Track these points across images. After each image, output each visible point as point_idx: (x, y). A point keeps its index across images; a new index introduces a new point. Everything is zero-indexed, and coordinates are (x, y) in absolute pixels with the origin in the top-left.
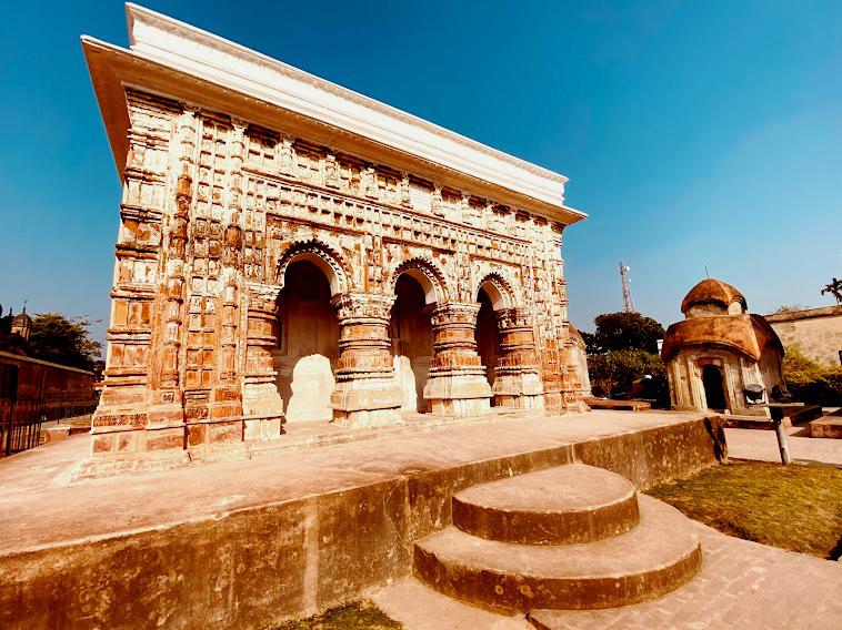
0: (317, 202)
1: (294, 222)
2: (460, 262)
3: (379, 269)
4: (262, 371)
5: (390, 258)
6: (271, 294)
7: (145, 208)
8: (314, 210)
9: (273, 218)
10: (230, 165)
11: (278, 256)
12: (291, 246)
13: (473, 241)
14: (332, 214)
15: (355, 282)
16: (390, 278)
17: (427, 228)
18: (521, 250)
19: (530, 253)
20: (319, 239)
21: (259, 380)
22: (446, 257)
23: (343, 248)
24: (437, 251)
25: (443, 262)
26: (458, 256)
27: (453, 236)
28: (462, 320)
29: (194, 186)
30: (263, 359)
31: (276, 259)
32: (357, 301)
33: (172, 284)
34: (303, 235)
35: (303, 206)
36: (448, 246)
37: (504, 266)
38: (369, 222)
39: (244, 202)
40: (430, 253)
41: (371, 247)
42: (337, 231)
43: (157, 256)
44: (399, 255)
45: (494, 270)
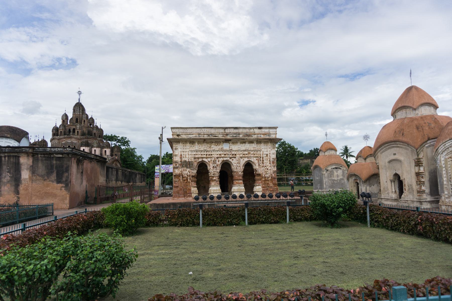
0: (203, 153)
1: (198, 158)
8: (202, 155)
9: (195, 158)
10: (187, 150)
11: (196, 165)
17: (228, 153)
19: (261, 153)
21: (195, 187)
22: (233, 159)
24: (231, 158)
27: (235, 153)
34: (200, 160)
36: (234, 156)
39: (190, 156)
42: (207, 158)
45: (249, 159)
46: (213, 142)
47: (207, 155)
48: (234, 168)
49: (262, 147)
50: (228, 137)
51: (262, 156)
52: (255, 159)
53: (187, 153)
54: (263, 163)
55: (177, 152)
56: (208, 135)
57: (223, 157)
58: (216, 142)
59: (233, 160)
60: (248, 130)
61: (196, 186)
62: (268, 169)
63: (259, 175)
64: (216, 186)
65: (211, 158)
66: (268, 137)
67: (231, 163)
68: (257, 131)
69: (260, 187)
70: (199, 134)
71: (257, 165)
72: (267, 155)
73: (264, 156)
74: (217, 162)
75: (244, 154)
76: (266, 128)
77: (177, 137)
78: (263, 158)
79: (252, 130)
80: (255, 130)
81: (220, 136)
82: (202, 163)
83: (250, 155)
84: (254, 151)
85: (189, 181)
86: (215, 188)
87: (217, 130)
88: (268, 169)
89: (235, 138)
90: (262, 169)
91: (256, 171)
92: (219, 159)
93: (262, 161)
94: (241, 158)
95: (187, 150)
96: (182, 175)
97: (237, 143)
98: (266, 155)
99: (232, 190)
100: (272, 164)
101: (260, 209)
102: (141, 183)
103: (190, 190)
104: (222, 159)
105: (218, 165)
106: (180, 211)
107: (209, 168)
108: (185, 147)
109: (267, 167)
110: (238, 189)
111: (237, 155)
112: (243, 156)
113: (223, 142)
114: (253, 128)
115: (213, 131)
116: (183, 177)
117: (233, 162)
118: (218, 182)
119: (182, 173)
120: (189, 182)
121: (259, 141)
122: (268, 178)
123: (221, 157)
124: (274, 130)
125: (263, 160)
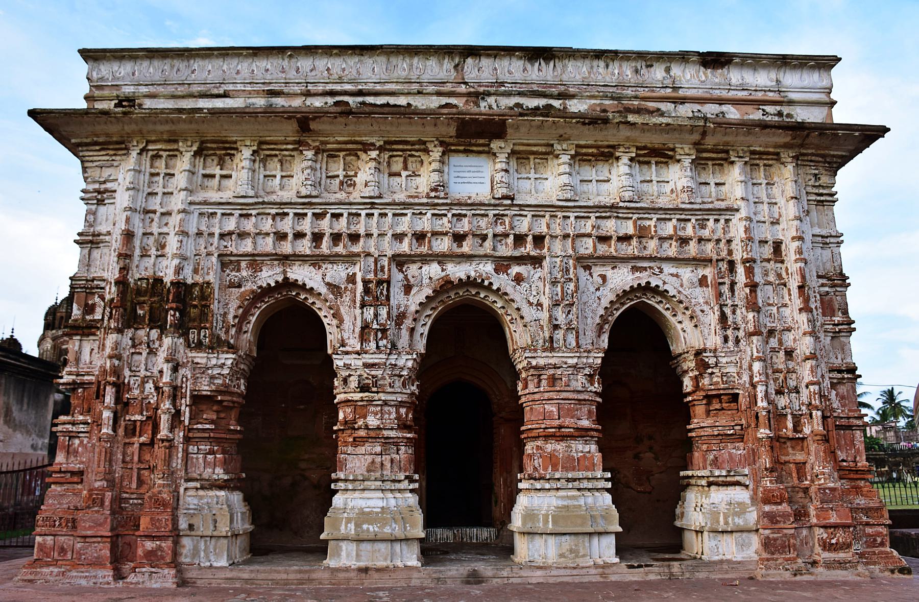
1: (256, 261)
3: (383, 312)
5: (408, 289)
10: (177, 202)
12: (253, 292)
13: (588, 230)
15: (346, 336)
16: (408, 322)
20: (292, 276)
23: (328, 284)
29: (137, 243)
31: (230, 317)
32: (347, 367)
34: (269, 276)
36: (529, 248)
37: (668, 268)
40: (488, 268)
41: (371, 276)
42: (316, 261)
45: (643, 278)
46: (366, 147)
52: (687, 273)
57: (442, 258)
59: (519, 279)
60: (625, 72)
61: (220, 474)
64: (387, 485)
68: (691, 78)
69: (741, 495)
72: (777, 246)
74: (397, 297)
76: (755, 61)
78: (749, 272)
80: (677, 70)
85: (164, 432)
86: (373, 501)
87: (403, 67)
88: (789, 354)
91: (703, 366)
92: (413, 269)
94: (585, 262)
96: (120, 388)
98: (768, 251)
99: (517, 522)
104: (434, 270)
107: (332, 336)
110: (561, 515)
112: (602, 249)
115: (371, 72)
116: (122, 405)
117: (517, 294)
118: (404, 453)
119: (116, 371)
121: (712, 146)
123: (425, 259)
124: (812, 79)
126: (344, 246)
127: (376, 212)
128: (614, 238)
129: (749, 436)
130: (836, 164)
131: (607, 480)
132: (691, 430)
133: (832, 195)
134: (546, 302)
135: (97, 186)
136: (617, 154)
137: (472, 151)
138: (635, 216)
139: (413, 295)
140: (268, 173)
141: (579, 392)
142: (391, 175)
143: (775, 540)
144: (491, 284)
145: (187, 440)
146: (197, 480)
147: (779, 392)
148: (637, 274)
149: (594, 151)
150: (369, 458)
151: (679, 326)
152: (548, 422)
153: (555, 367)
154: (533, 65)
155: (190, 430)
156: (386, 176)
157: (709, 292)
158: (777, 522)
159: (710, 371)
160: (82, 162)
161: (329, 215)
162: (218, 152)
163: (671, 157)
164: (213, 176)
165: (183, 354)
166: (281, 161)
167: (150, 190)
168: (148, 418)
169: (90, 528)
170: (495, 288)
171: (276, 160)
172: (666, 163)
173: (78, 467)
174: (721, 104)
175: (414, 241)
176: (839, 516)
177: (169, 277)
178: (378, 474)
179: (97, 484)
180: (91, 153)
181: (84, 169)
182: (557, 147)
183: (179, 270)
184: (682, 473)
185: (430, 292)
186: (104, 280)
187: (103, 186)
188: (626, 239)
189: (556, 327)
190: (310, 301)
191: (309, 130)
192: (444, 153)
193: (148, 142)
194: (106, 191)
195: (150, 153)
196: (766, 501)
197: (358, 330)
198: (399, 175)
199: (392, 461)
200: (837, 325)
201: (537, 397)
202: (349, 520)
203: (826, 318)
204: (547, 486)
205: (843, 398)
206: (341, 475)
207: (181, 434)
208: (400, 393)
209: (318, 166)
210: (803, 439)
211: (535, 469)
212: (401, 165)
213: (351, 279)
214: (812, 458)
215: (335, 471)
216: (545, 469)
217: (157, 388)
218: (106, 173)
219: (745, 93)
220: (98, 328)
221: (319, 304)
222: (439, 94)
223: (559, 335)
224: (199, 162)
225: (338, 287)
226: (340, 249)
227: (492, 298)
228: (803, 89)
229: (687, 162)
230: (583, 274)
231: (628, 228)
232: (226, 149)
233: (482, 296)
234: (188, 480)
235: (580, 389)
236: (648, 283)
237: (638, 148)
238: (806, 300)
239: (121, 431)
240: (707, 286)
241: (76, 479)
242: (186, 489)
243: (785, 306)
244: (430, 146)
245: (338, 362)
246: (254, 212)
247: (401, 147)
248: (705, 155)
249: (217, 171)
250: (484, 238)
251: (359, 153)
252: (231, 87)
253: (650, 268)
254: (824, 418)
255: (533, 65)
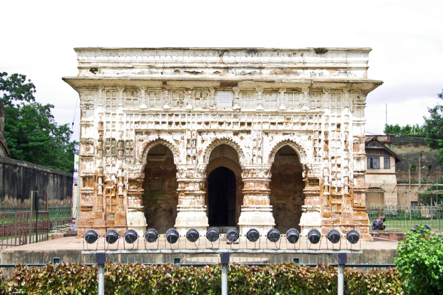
0: (160, 119)
1: (148, 133)
2: (255, 137)
3: (194, 151)
4: (135, 206)
5: (203, 141)
6: (138, 169)
7: (88, 138)
8: (157, 123)
11: (141, 150)
12: (147, 143)
14: (167, 123)
16: (203, 154)
18: (315, 120)
19: (323, 120)
23: (175, 140)
24: (236, 133)
25: (242, 138)
26: (254, 134)
27: (249, 120)
28: (254, 176)
29: (105, 124)
30: (136, 201)
32: (182, 170)
33: (99, 170)
34: (153, 137)
35: (152, 122)
36: (246, 127)
38: (189, 123)
39: (125, 127)
41: (189, 138)
42: (170, 132)
43: (93, 158)
44: (209, 138)
45: (287, 137)
46: (187, 89)
47: (170, 123)
48: (245, 161)
49: (326, 104)
50: (230, 76)
51: (323, 130)
53: (117, 117)
54: (327, 150)
55: (95, 116)
56: (176, 70)
57: (214, 132)
58: (195, 89)
61: (139, 206)
62: (339, 166)
63: (315, 181)
65: (182, 131)
66: (341, 76)
67: (238, 146)
70: (151, 67)
71: (310, 153)
72: (339, 126)
73: (330, 129)
75: (273, 124)
76: (337, 51)
77: (91, 75)
79: (297, 58)
81: (209, 74)
82: (161, 145)
83: (290, 127)
84: (304, 115)
86: (191, 215)
88: (339, 166)
89: (249, 77)
90: (324, 163)
92: (204, 136)
93: (323, 143)
94: (267, 133)
95: (119, 110)
96: (103, 178)
97: (254, 91)
98: (335, 127)
100: (351, 152)
101: (267, 273)
102: (62, 199)
103: (124, 217)
105: (201, 151)
106: (50, 269)
108: (111, 102)
109: (339, 161)
111: (254, 127)
112: (272, 127)
113: (216, 89)
114: (302, 52)
115: (187, 59)
119: (102, 172)
120: (122, 196)
122: (339, 189)
123: (208, 131)
125: (327, 142)
126: (180, 127)
127: (191, 114)
128: (277, 123)
129: (321, 194)
130: (365, 93)
131: (271, 208)
132: (305, 191)
133: (364, 104)
134: (252, 147)
135: (85, 102)
136: (279, 91)
137: (226, 90)
138: (285, 115)
139: (204, 145)
140: (151, 98)
141: (262, 178)
142: (196, 99)
143: (326, 229)
144: (232, 140)
145: (128, 195)
146: (132, 208)
147: (333, 180)
148: (285, 136)
149: (271, 90)
150: (190, 200)
151: (300, 154)
152: (251, 189)
153: (254, 170)
154: (249, 54)
155: (129, 192)
156: (194, 100)
157: (311, 142)
158: (327, 223)
159: (309, 171)
160: (79, 93)
161: (174, 115)
162: (132, 90)
163: (301, 91)
164: (130, 99)
165: (125, 166)
166: (155, 94)
167: (107, 105)
168: (114, 188)
169: (98, 225)
170: (233, 141)
171: (153, 93)
172: (299, 93)
173: (90, 205)
174: (322, 69)
175: (205, 125)
176: (349, 222)
177: (117, 139)
178: (193, 206)
179: (99, 211)
180: (83, 90)
181: (80, 96)
182: (257, 89)
183: (121, 136)
184: (303, 206)
185: (210, 143)
186: (93, 139)
187: (88, 103)
188: (281, 123)
189: (254, 155)
190: (168, 145)
191: (166, 84)
192: (215, 91)
193: (105, 87)
194: (90, 104)
195: (106, 91)
196: (324, 216)
197: (185, 156)
198: (199, 99)
199: (198, 201)
200: (359, 155)
201: (247, 180)
202: (184, 221)
203: (354, 152)
204: (250, 210)
205: (359, 181)
206: (181, 206)
207: (126, 193)
208: (200, 177)
209: (169, 96)
210: (341, 196)
211: (246, 204)
212: (199, 95)
213: (183, 138)
214: (343, 202)
215: (178, 204)
216: (249, 204)
217: (116, 177)
218: (89, 97)
219: (333, 64)
220: (93, 157)
221: (171, 146)
222: (214, 68)
223: (255, 158)
224: (125, 94)
225: (178, 141)
226: (178, 127)
227: (233, 144)
228: (356, 62)
229: (306, 93)
230: (265, 137)
231: (282, 120)
232: (134, 89)
233: (229, 143)
234: (129, 208)
235: (262, 177)
236: (289, 140)
237: (287, 89)
238: (347, 146)
239: (104, 192)
240: (311, 140)
241: (90, 209)
242: (128, 212)
243: (339, 148)
244: (210, 89)
245: (179, 168)
246: (147, 114)
247: (199, 89)
248: (313, 90)
249: (132, 98)
250: (230, 123)
251: (184, 91)
252: (135, 64)
253: (290, 134)
254: (349, 188)
255: (249, 54)
